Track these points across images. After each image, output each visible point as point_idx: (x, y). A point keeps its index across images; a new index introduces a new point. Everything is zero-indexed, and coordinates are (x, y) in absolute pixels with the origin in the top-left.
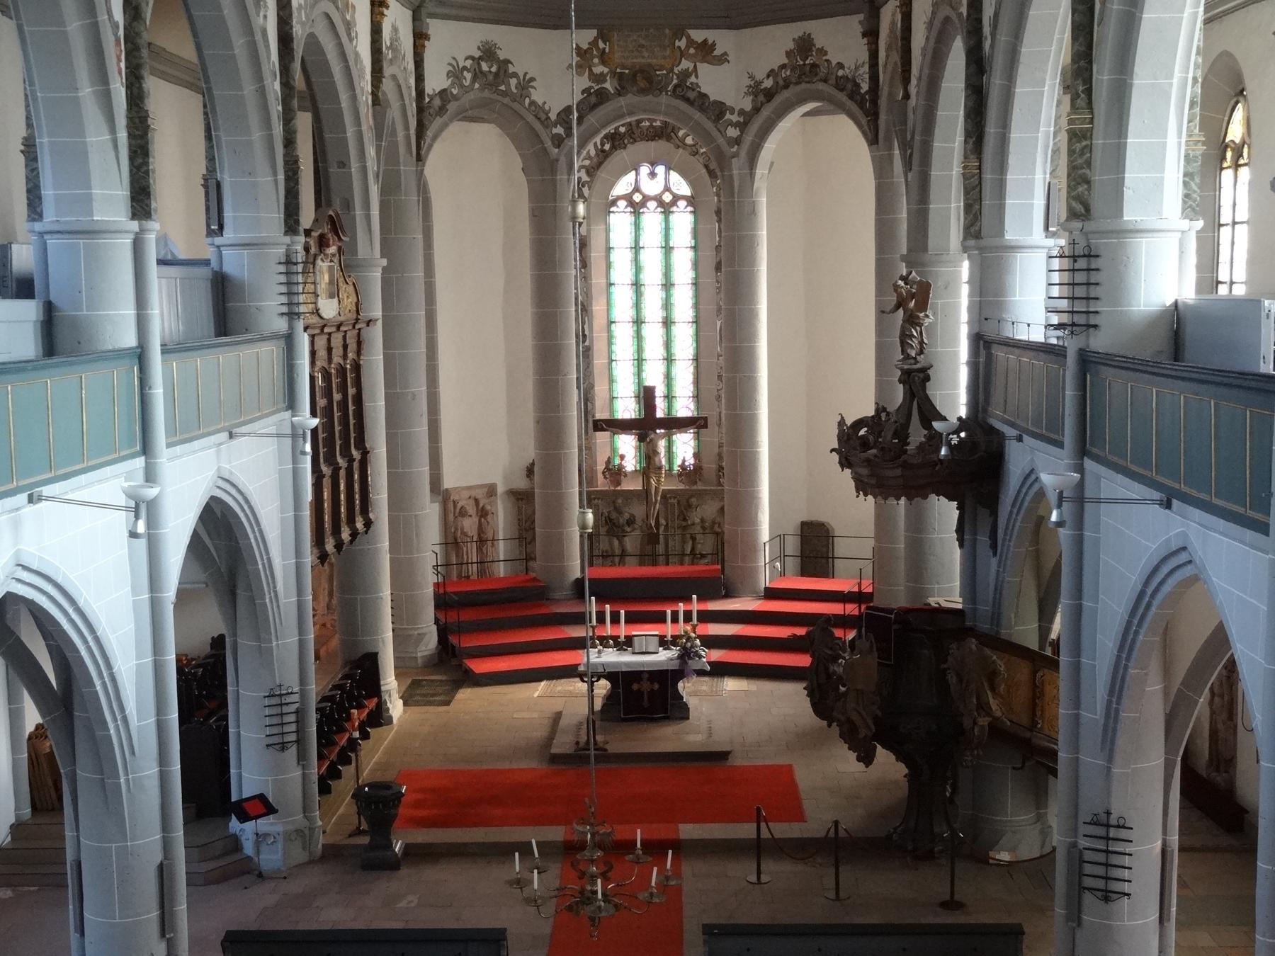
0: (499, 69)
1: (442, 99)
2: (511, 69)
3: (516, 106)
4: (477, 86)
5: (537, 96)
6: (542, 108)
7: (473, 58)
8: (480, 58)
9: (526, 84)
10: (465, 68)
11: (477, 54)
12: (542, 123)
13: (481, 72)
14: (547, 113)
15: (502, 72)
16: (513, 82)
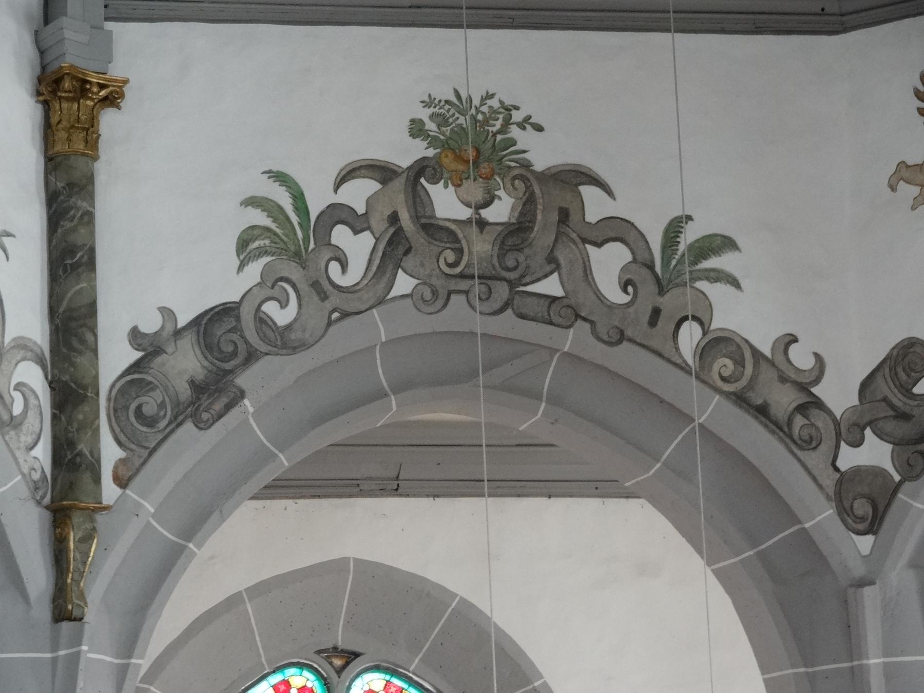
0: (528, 205)
1: (208, 345)
2: (595, 206)
3: (628, 360)
4: (404, 284)
5: (747, 312)
6: (775, 362)
7: (383, 172)
8: (421, 169)
9: (677, 266)
10: (338, 214)
11: (406, 153)
12: (780, 428)
13: (433, 229)
14: (805, 386)
15: (546, 219)
16: (608, 264)
